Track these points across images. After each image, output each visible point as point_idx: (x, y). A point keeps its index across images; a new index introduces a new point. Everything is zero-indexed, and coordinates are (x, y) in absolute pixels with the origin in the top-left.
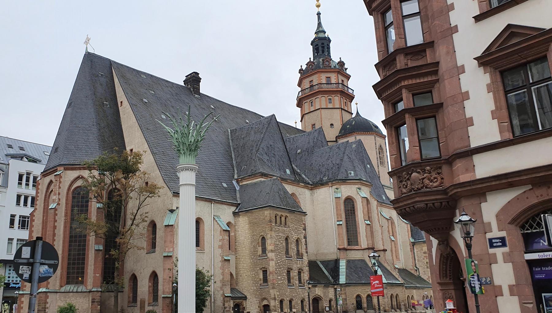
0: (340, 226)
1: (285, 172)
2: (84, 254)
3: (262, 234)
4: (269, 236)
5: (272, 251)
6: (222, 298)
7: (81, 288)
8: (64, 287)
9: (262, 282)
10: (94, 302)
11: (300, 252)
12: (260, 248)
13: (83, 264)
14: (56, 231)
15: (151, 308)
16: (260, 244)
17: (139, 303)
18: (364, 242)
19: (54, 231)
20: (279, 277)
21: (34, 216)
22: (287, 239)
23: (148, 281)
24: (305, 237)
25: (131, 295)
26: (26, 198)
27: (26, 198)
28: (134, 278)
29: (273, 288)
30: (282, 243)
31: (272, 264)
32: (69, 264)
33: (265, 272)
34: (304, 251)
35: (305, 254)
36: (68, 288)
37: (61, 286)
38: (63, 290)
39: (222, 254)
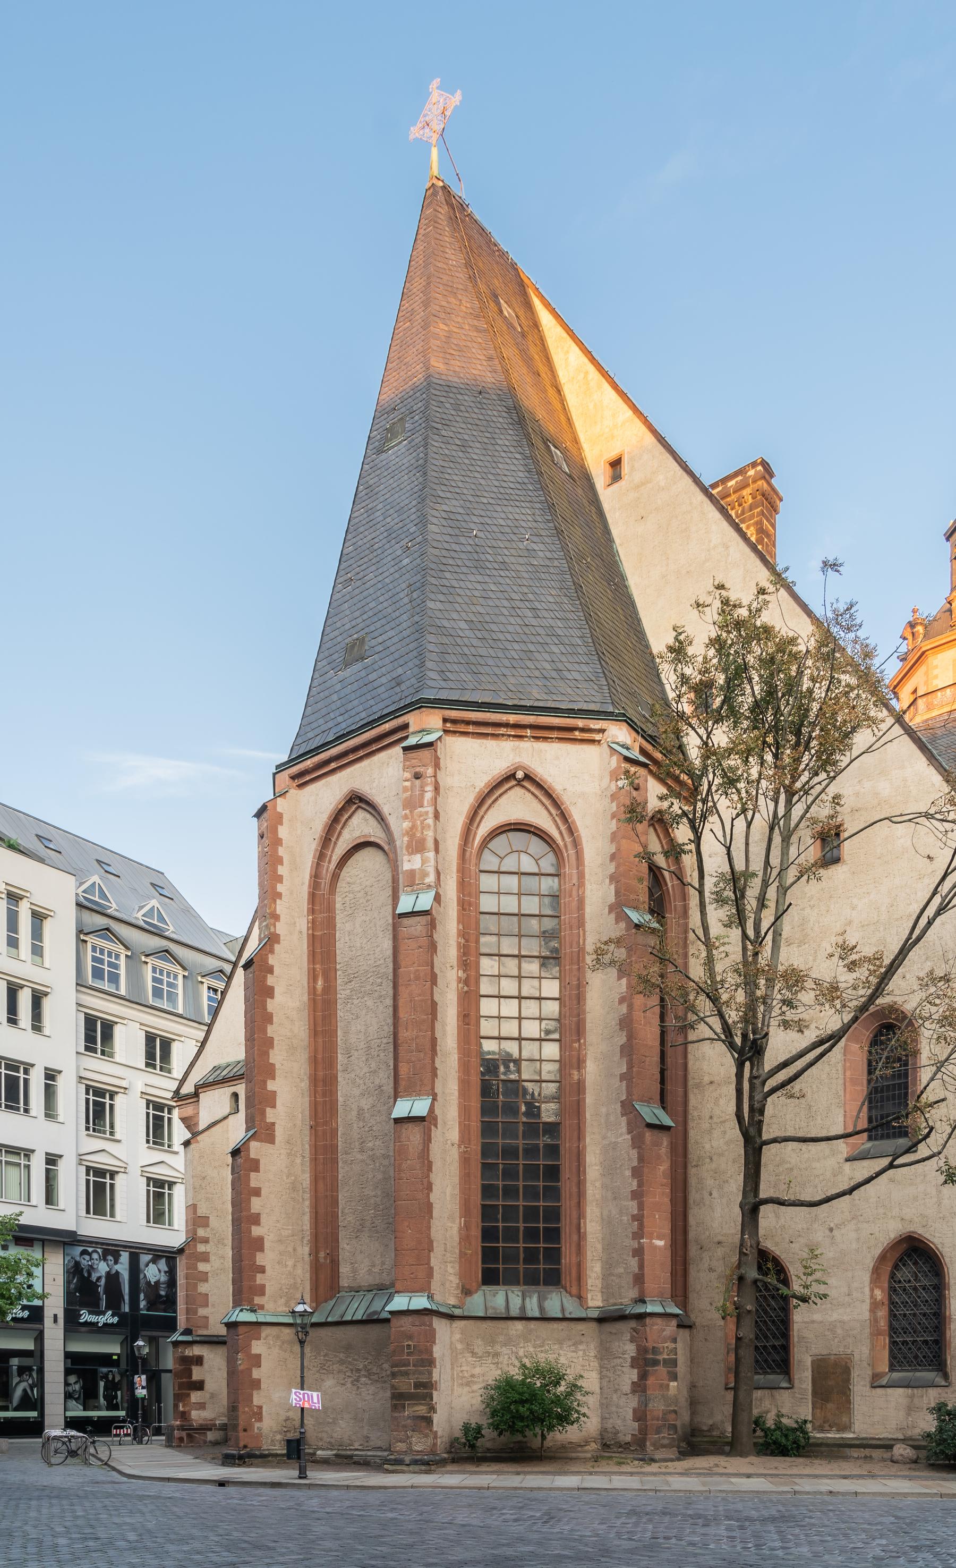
7: (555, 1302)
10: (655, 1363)
21: (271, 970)
23: (866, 1277)
36: (500, 1298)
38: (476, 1303)
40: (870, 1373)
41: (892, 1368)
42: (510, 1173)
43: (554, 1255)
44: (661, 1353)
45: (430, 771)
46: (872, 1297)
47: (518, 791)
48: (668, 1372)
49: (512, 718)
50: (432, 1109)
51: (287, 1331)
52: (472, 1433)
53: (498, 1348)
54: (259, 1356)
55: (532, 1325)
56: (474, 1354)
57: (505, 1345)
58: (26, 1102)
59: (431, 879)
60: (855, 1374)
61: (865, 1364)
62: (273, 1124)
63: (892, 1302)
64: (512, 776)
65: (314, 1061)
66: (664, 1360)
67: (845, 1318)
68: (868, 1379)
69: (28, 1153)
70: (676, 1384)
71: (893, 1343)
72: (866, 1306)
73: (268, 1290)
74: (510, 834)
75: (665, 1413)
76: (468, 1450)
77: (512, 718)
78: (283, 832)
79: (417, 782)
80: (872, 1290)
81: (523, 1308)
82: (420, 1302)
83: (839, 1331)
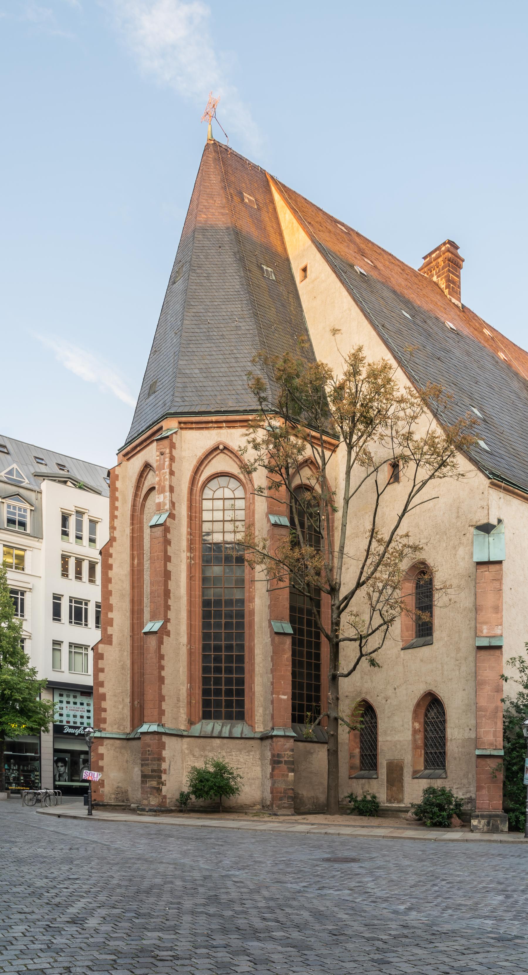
2: (241, 647)
7: (239, 729)
13: (241, 670)
17: (383, 771)
25: (357, 751)
26: (79, 563)
27: (79, 563)
28: (367, 710)
32: (205, 670)
40: (412, 770)
41: (426, 768)
42: (217, 659)
43: (241, 704)
44: (283, 757)
45: (168, 451)
46: (413, 727)
47: (222, 455)
48: (288, 768)
49: (214, 418)
51: (118, 742)
52: (184, 799)
53: (207, 753)
54: (102, 754)
55: (225, 741)
56: (194, 756)
57: (210, 751)
58: (86, 621)
59: (167, 507)
60: (405, 770)
61: (409, 765)
62: (112, 635)
63: (426, 730)
64: (217, 448)
65: (133, 601)
66: (285, 761)
67: (401, 739)
68: (411, 774)
69: (86, 647)
70: (293, 774)
71: (426, 753)
72: (410, 733)
73: (108, 721)
74: (219, 479)
75: (285, 790)
76: (183, 806)
77: (214, 418)
78: (118, 484)
79: (162, 457)
80: (413, 723)
81: (221, 732)
83: (398, 746)
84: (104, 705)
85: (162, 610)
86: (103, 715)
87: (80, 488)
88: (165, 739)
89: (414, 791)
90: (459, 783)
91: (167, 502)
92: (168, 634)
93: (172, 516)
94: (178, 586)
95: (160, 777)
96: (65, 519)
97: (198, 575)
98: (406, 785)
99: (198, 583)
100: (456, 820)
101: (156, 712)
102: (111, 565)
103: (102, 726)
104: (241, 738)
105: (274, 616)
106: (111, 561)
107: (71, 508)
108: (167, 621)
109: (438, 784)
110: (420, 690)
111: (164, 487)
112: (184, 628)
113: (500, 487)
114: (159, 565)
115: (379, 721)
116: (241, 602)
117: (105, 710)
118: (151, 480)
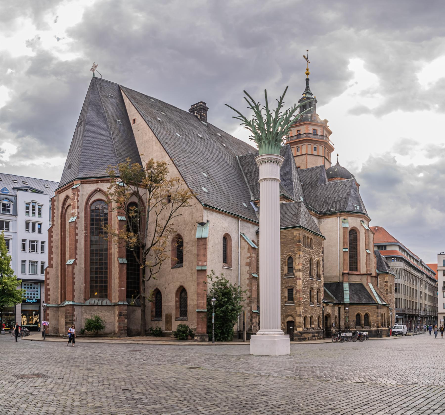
0: (346, 253)
1: (300, 199)
2: (106, 268)
3: (290, 254)
4: (297, 256)
5: (299, 270)
6: (249, 314)
8: (88, 301)
9: (287, 299)
10: (121, 315)
11: (319, 273)
12: (287, 267)
13: (106, 277)
14: (78, 245)
15: (179, 323)
16: (287, 264)
17: (164, 318)
18: (363, 269)
19: (76, 245)
20: (304, 296)
22: (310, 261)
24: (323, 260)
25: (154, 309)
28: (158, 293)
29: (299, 305)
30: (307, 264)
31: (300, 282)
32: (91, 278)
33: (290, 291)
34: (321, 272)
35: (322, 276)
36: (92, 301)
37: (85, 300)
38: (87, 303)
39: (249, 272)
41: (180, 316)
43: (106, 291)
50: (75, 262)
51: (55, 308)
53: (92, 312)
54: (48, 314)
55: (99, 307)
56: (87, 313)
57: (93, 311)
63: (180, 301)
71: (181, 310)
73: (51, 300)
75: (124, 327)
81: (98, 303)
82: (71, 303)
84: (49, 293)
85: (74, 255)
86: (49, 297)
87: (33, 192)
88: (75, 307)
89: (175, 325)
90: (192, 323)
91: (76, 212)
92: (76, 264)
93: (78, 218)
94: (80, 245)
95: (73, 323)
96: (27, 208)
97: (89, 240)
98: (173, 323)
99: (89, 243)
100: (189, 337)
101: (71, 296)
102: (53, 236)
103: (48, 302)
104: (106, 306)
105: (120, 256)
106: (52, 234)
107: (29, 201)
108: (76, 259)
109: (184, 323)
110: (178, 285)
111: (75, 207)
112: (83, 261)
113: (208, 209)
114: (73, 237)
115: (163, 297)
116: (106, 250)
117: (50, 295)
118: (69, 202)
